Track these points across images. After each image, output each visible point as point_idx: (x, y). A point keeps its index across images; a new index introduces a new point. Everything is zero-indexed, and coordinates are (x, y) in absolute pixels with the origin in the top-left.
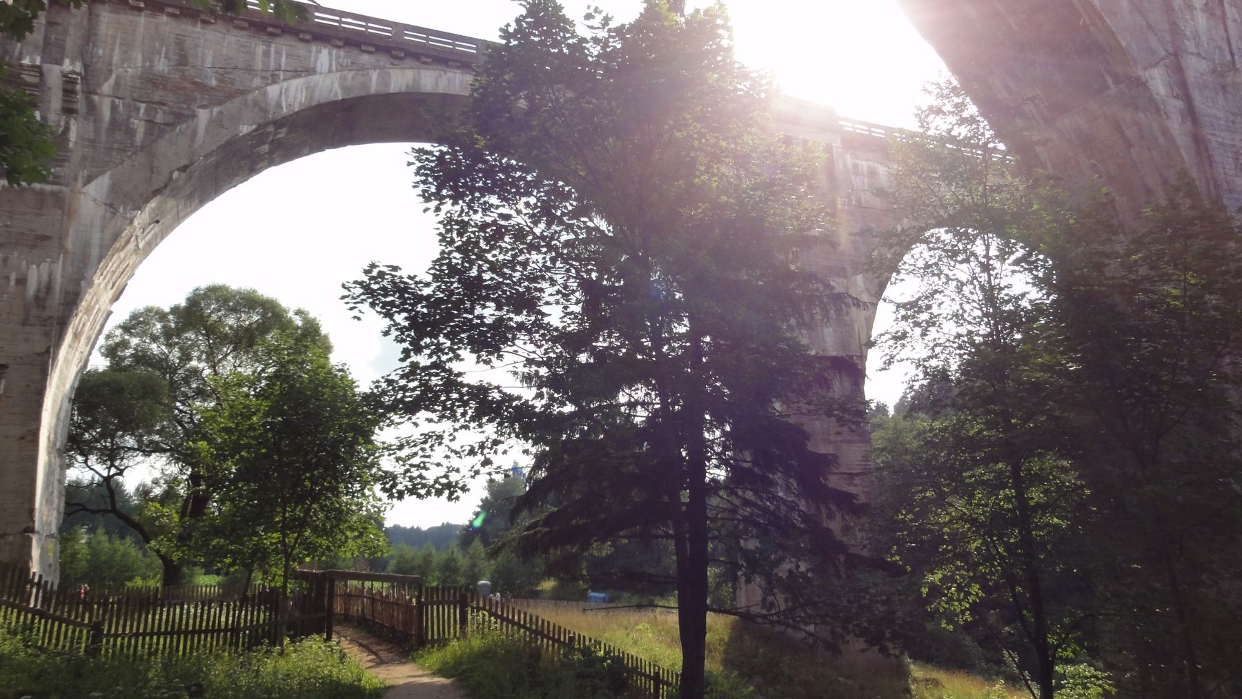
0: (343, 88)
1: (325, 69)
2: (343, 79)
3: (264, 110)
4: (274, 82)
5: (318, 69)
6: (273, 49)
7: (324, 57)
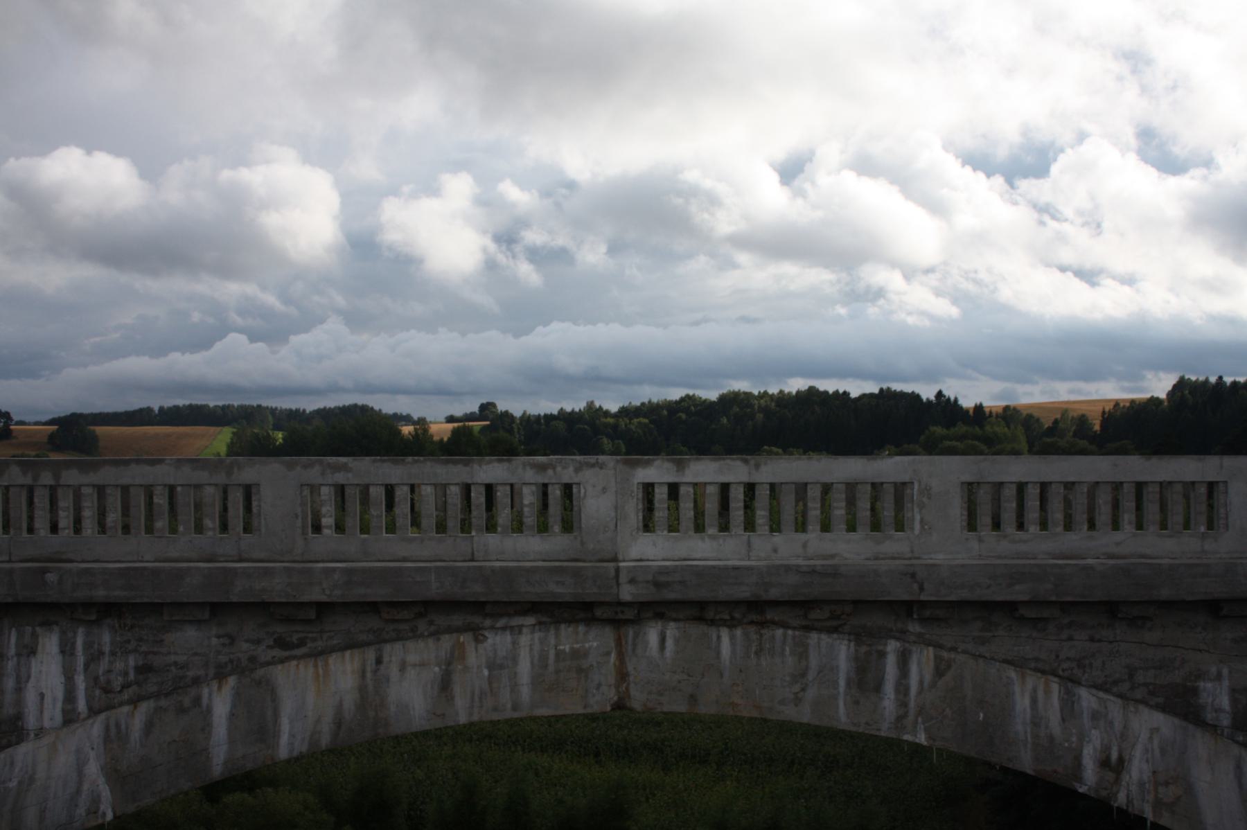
1: (53, 713)
2: (114, 738)
5: (31, 721)
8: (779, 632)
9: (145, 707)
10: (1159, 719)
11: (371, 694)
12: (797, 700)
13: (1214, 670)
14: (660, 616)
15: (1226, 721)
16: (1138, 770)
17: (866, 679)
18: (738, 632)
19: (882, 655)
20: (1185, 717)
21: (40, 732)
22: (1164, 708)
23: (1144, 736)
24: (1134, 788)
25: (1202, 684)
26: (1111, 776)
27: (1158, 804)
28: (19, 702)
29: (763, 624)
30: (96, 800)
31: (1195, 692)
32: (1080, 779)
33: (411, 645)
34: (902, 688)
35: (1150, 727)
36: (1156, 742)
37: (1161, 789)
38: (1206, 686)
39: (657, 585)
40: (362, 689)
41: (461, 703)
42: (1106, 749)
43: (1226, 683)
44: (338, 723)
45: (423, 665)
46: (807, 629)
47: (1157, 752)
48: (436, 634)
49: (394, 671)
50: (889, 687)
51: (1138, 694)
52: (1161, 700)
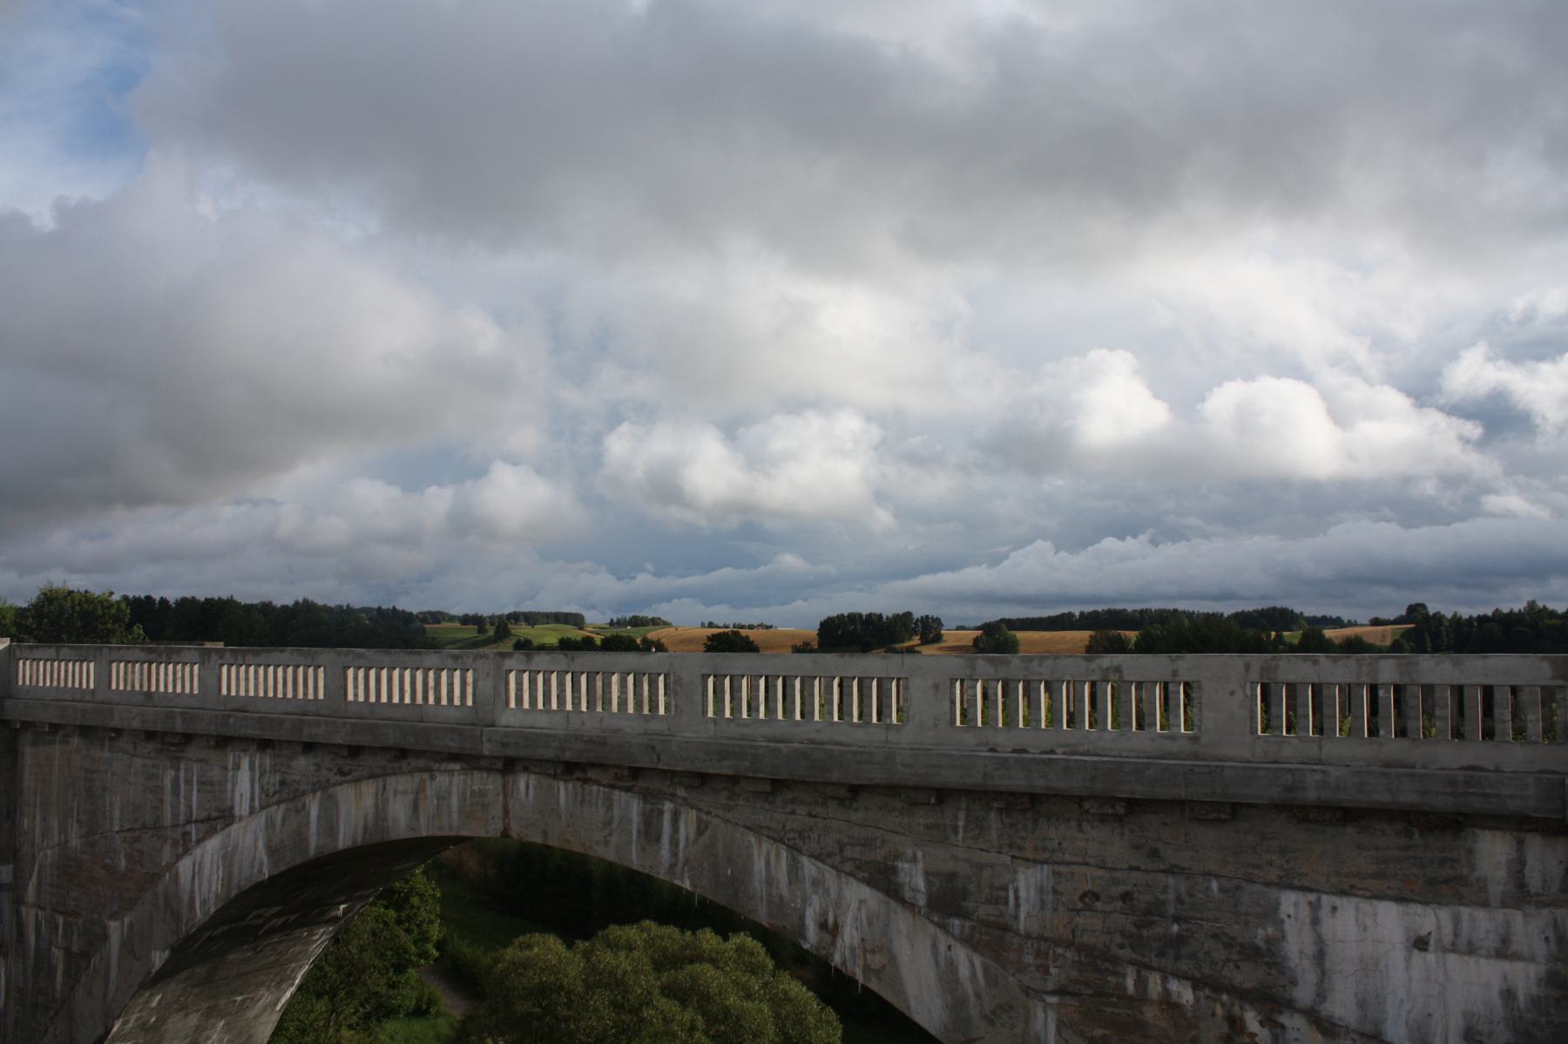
0: (272, 851)
2: (270, 825)
3: (176, 916)
4: (186, 851)
5: (237, 812)
6: (182, 774)
7: (244, 780)
8: (595, 788)
9: (283, 807)
10: (866, 892)
11: (380, 812)
12: (606, 843)
13: (909, 852)
14: (526, 769)
15: (922, 901)
16: (849, 935)
17: (650, 833)
18: (570, 785)
19: (661, 812)
20: (887, 893)
21: (241, 818)
22: (869, 882)
23: (854, 906)
24: (847, 952)
25: (900, 864)
26: (828, 938)
27: (867, 969)
28: (233, 799)
29: (586, 781)
30: (261, 865)
31: (894, 870)
32: (804, 938)
33: (399, 778)
34: (674, 842)
35: (858, 897)
36: (864, 911)
37: (869, 956)
38: (903, 866)
39: (504, 745)
40: (376, 806)
41: (423, 821)
42: (824, 913)
43: (921, 866)
44: (366, 829)
45: (404, 793)
46: (613, 787)
47: (865, 922)
48: (411, 772)
49: (391, 795)
50: (665, 840)
51: (848, 867)
52: (866, 875)
